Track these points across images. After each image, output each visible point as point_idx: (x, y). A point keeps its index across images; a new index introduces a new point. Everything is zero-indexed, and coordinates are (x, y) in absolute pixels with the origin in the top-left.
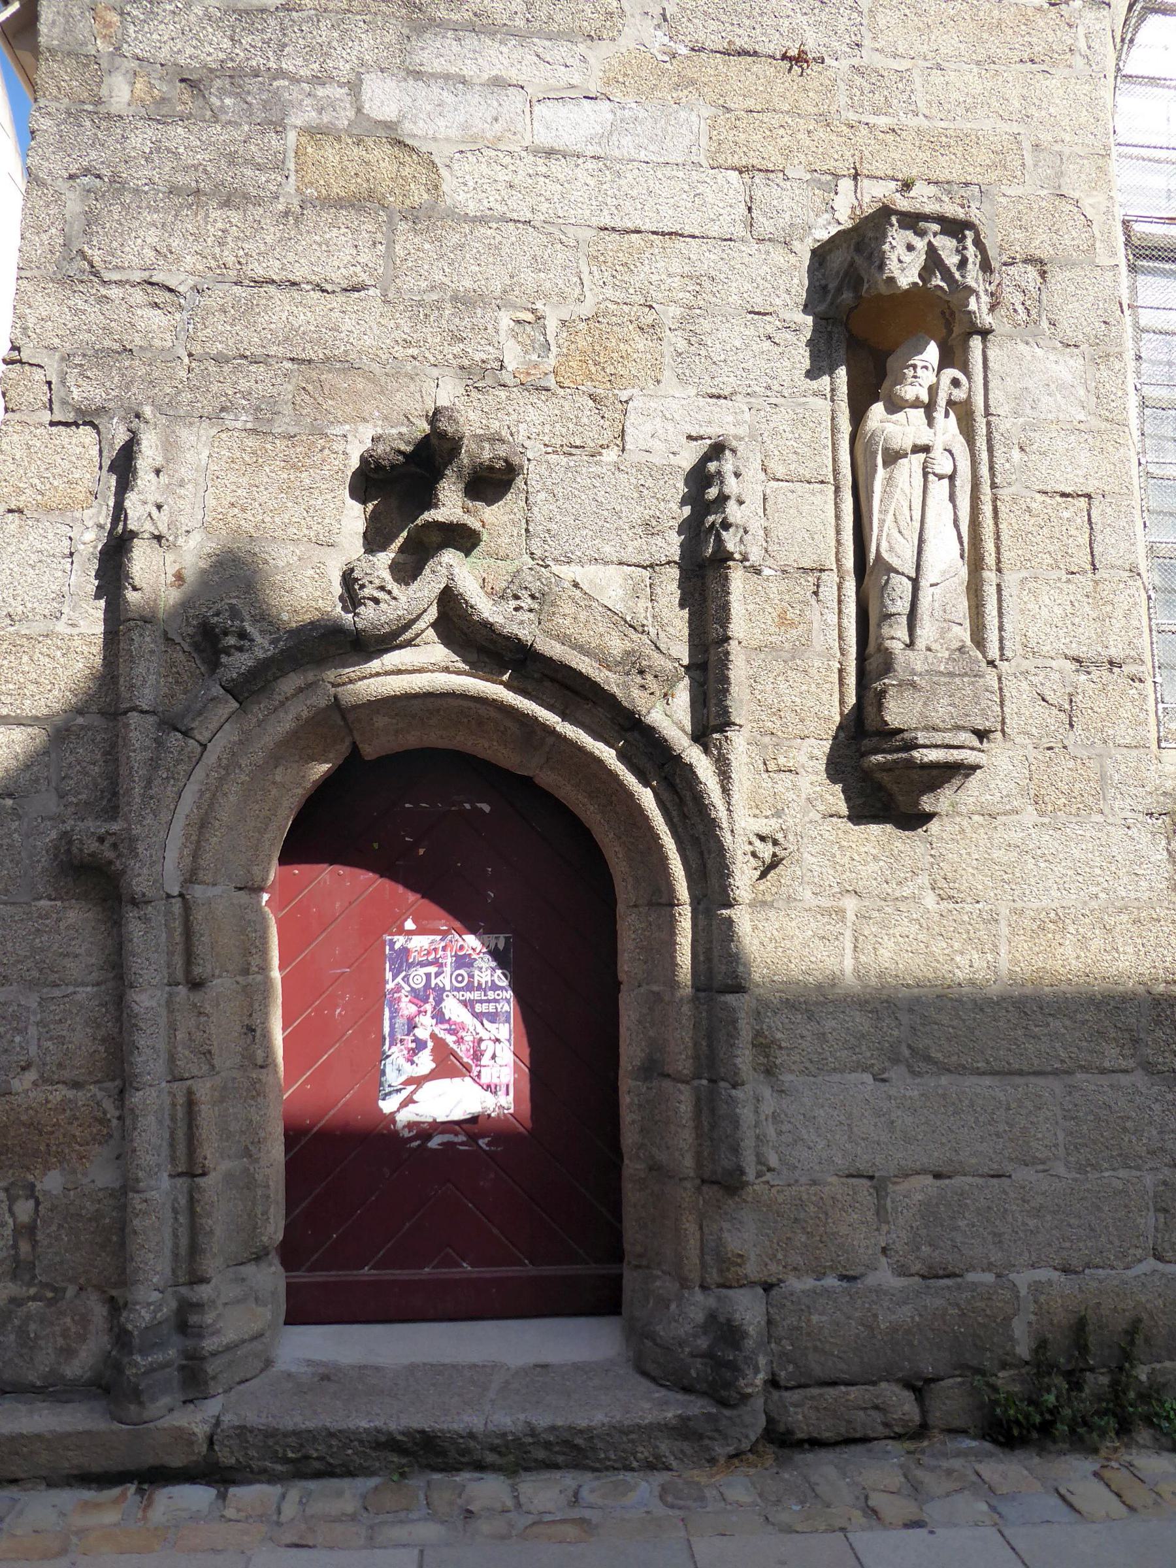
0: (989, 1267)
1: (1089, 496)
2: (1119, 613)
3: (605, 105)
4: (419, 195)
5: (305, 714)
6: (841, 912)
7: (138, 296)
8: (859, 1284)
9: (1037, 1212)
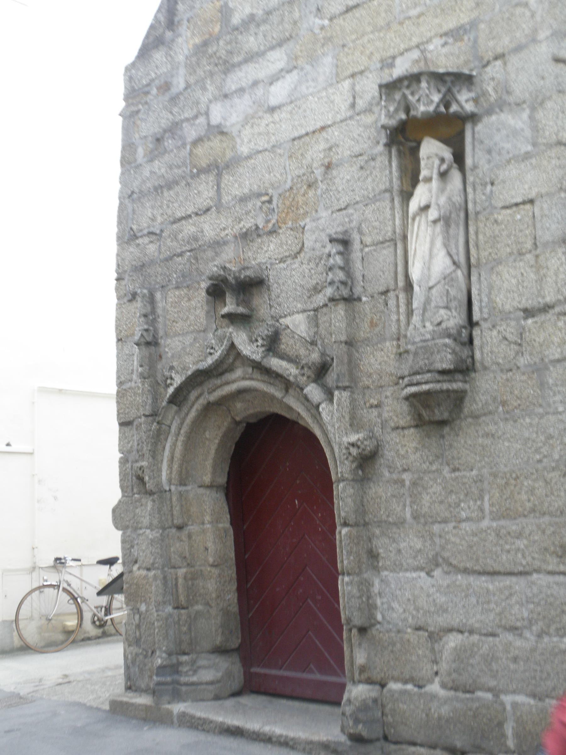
0: (489, 690)
1: (531, 202)
2: (551, 273)
3: (295, 72)
4: (229, 154)
5: (199, 408)
6: (402, 482)
7: (146, 240)
8: (423, 690)
9: (515, 660)
